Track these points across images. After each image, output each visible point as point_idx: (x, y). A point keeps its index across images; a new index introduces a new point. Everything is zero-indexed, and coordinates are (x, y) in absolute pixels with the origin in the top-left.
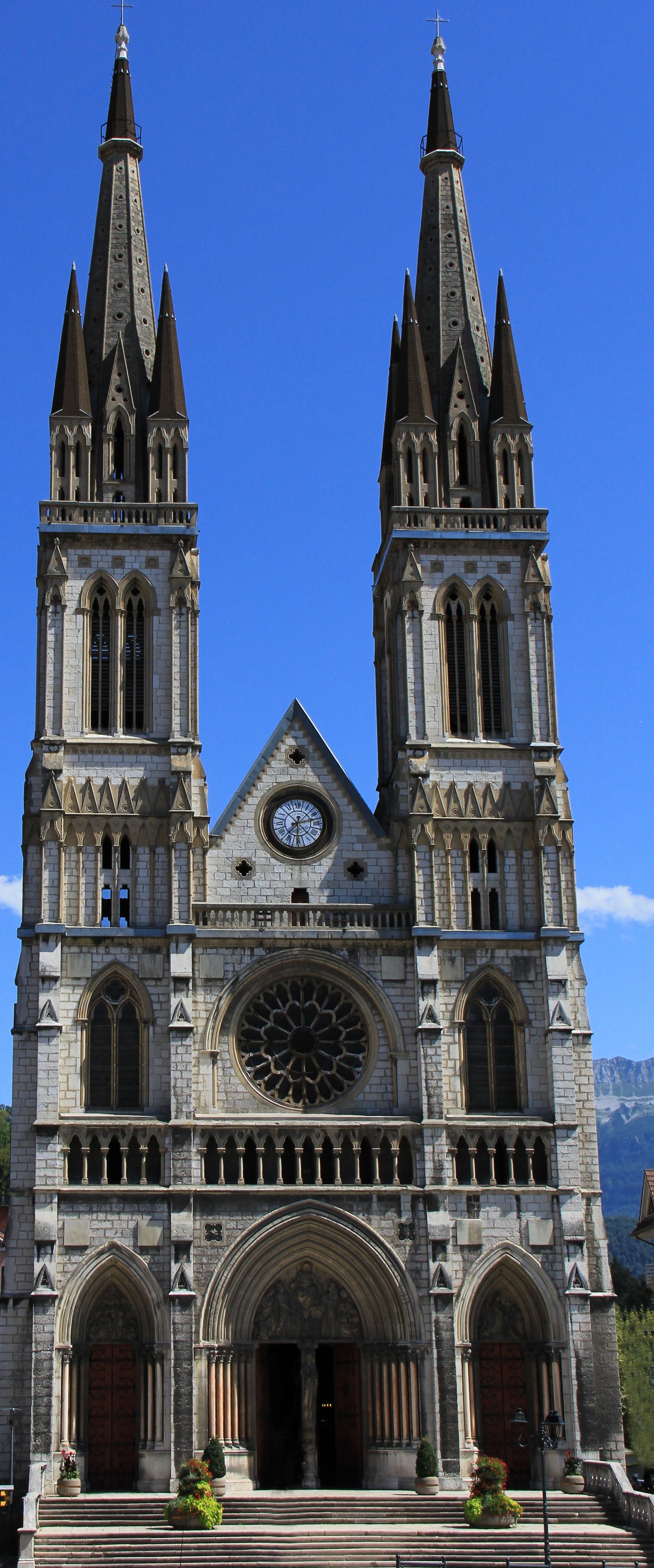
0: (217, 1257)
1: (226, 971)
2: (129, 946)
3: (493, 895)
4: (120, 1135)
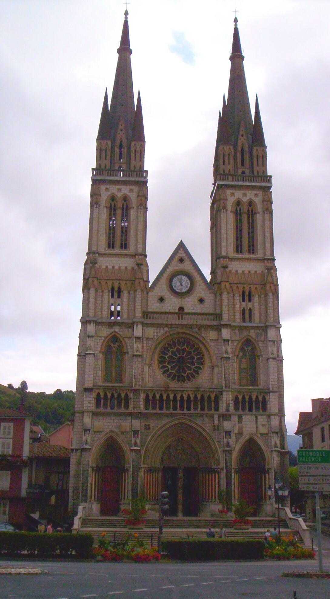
1: (154, 336)
2: (119, 325)
3: (250, 310)
4: (114, 392)
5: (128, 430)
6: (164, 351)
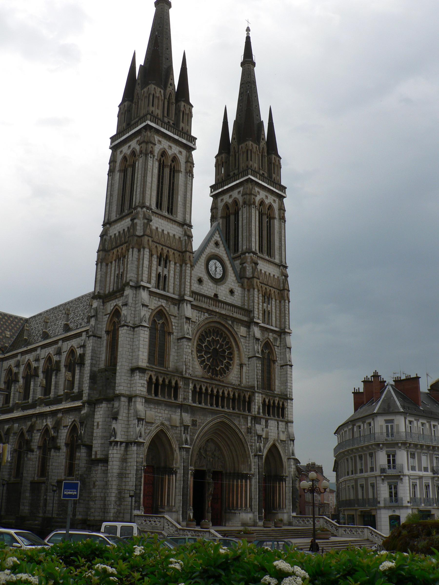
2: (166, 300)
4: (166, 378)
5: (178, 425)
6: (201, 339)
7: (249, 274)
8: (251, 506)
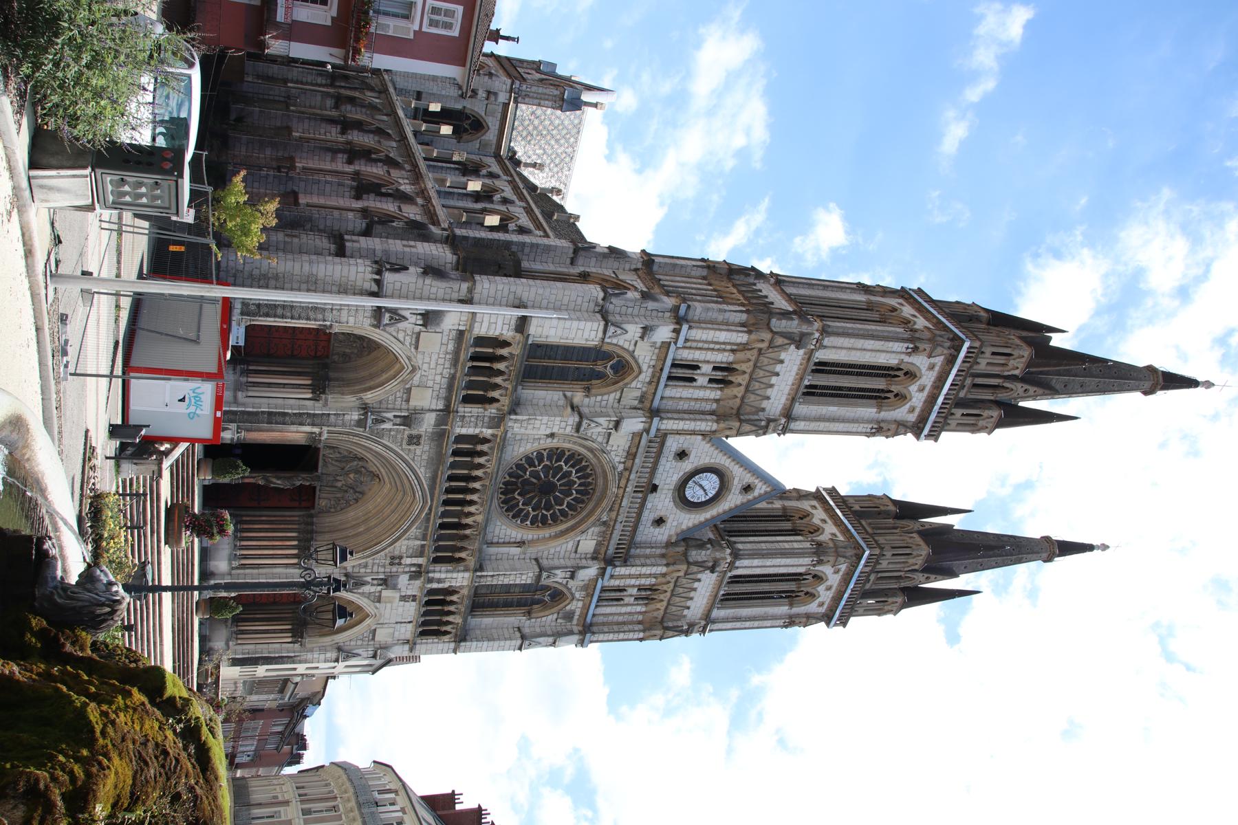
0: (394, 442)
2: (650, 383)
5: (413, 403)
6: (575, 459)
7: (696, 555)
8: (243, 566)
